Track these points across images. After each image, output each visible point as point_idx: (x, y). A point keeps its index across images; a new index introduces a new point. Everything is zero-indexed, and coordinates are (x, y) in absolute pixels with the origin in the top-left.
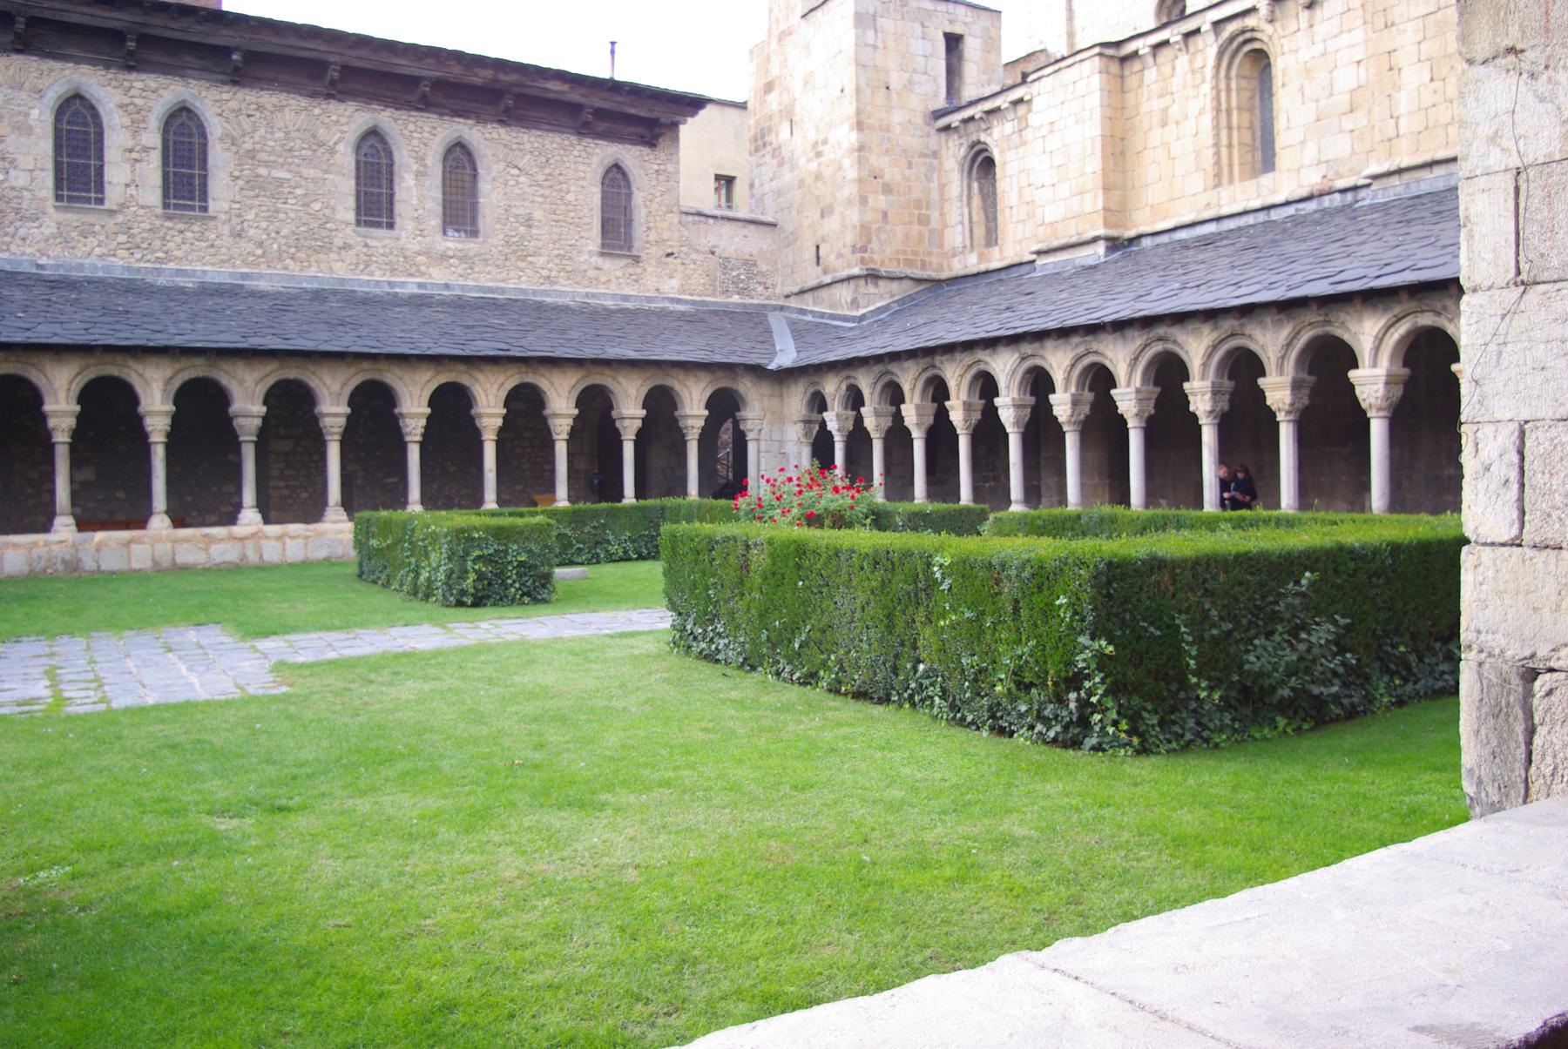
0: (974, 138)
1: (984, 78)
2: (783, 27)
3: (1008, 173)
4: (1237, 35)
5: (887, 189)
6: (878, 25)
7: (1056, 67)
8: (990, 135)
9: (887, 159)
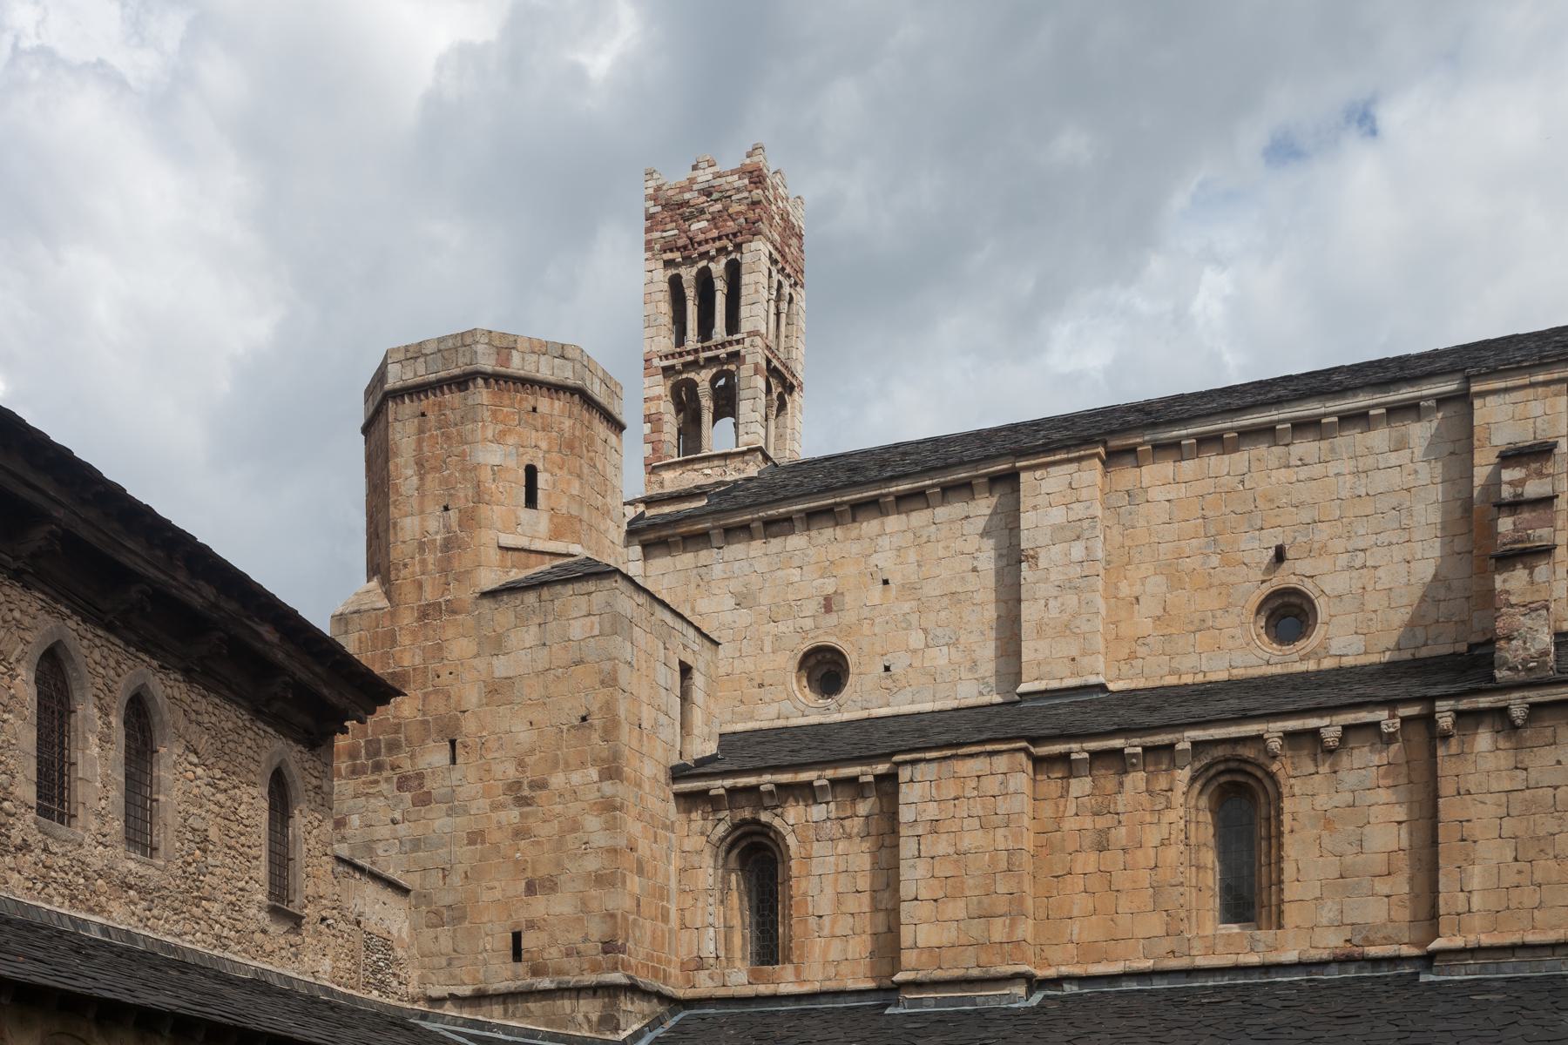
0: (747, 814)
2: (429, 595)
3: (815, 871)
5: (640, 871)
6: (635, 636)
7: (949, 753)
8: (781, 816)
9: (639, 825)
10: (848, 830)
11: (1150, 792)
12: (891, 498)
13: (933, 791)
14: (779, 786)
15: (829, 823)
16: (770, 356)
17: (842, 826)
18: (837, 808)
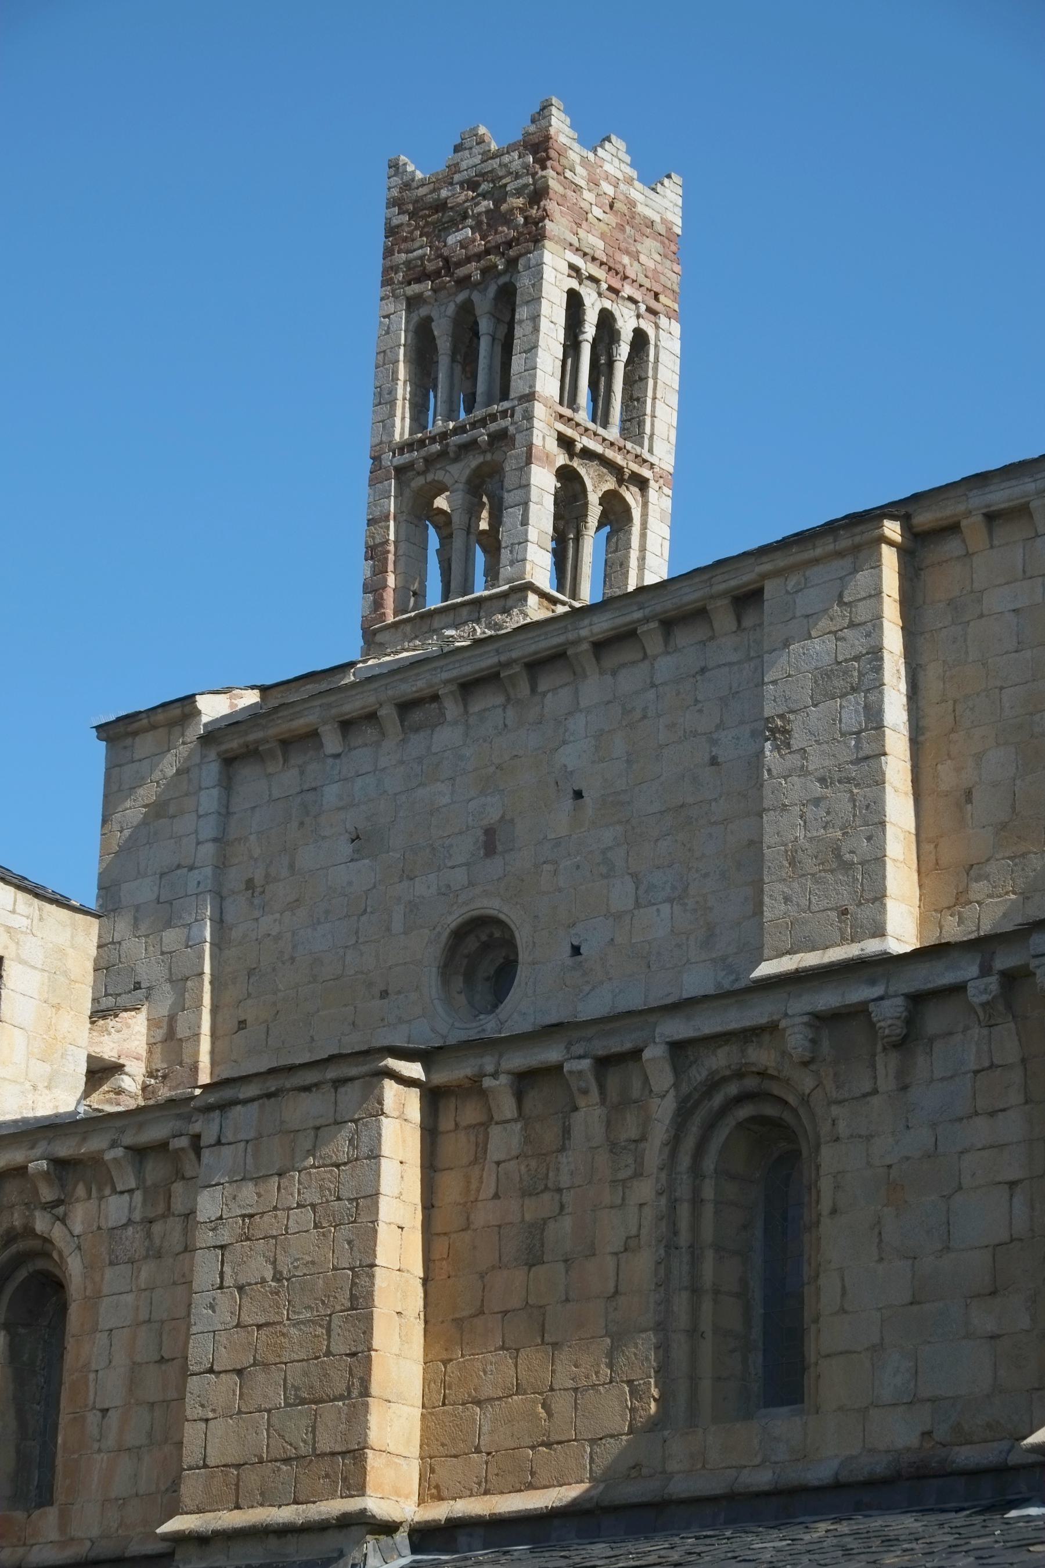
0: (17, 1222)
1: (41, 1069)
4: (725, 1080)
7: (272, 1085)
8: (63, 1220)
10: (157, 1241)
11: (614, 1147)
12: (585, 646)
13: (250, 1160)
14: (60, 1165)
15: (130, 1229)
16: (569, 432)
17: (149, 1235)
18: (145, 1202)
